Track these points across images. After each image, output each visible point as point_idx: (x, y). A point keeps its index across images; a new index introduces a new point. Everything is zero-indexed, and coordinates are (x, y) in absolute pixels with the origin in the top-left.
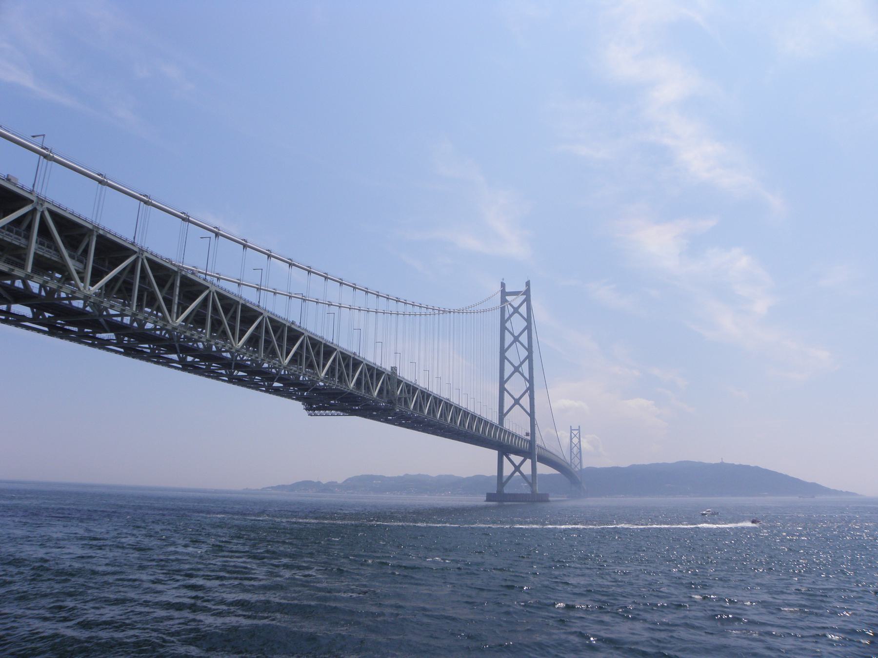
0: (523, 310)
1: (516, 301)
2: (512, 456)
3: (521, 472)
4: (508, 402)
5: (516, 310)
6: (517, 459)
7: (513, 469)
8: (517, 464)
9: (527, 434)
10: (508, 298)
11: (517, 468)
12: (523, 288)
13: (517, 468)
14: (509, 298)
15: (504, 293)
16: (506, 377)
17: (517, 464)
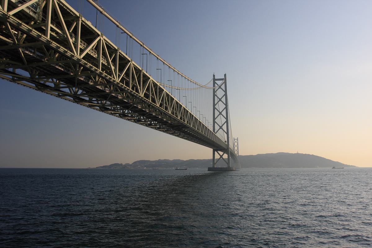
0: (223, 87)
1: (219, 83)
2: (220, 152)
3: (223, 158)
4: (217, 128)
5: (220, 87)
6: (221, 153)
7: (219, 157)
8: (221, 155)
9: (225, 142)
10: (216, 81)
11: (221, 156)
12: (223, 77)
13: (221, 156)
14: (216, 81)
15: (214, 80)
16: (216, 116)
17: (221, 155)
